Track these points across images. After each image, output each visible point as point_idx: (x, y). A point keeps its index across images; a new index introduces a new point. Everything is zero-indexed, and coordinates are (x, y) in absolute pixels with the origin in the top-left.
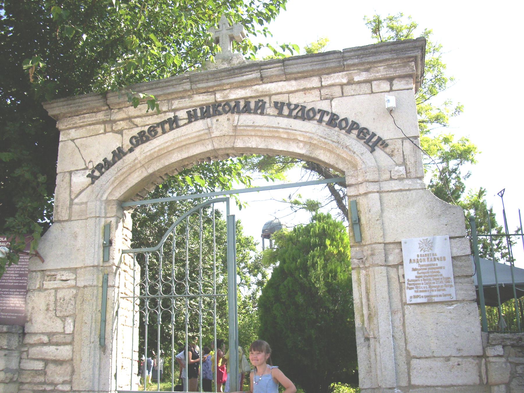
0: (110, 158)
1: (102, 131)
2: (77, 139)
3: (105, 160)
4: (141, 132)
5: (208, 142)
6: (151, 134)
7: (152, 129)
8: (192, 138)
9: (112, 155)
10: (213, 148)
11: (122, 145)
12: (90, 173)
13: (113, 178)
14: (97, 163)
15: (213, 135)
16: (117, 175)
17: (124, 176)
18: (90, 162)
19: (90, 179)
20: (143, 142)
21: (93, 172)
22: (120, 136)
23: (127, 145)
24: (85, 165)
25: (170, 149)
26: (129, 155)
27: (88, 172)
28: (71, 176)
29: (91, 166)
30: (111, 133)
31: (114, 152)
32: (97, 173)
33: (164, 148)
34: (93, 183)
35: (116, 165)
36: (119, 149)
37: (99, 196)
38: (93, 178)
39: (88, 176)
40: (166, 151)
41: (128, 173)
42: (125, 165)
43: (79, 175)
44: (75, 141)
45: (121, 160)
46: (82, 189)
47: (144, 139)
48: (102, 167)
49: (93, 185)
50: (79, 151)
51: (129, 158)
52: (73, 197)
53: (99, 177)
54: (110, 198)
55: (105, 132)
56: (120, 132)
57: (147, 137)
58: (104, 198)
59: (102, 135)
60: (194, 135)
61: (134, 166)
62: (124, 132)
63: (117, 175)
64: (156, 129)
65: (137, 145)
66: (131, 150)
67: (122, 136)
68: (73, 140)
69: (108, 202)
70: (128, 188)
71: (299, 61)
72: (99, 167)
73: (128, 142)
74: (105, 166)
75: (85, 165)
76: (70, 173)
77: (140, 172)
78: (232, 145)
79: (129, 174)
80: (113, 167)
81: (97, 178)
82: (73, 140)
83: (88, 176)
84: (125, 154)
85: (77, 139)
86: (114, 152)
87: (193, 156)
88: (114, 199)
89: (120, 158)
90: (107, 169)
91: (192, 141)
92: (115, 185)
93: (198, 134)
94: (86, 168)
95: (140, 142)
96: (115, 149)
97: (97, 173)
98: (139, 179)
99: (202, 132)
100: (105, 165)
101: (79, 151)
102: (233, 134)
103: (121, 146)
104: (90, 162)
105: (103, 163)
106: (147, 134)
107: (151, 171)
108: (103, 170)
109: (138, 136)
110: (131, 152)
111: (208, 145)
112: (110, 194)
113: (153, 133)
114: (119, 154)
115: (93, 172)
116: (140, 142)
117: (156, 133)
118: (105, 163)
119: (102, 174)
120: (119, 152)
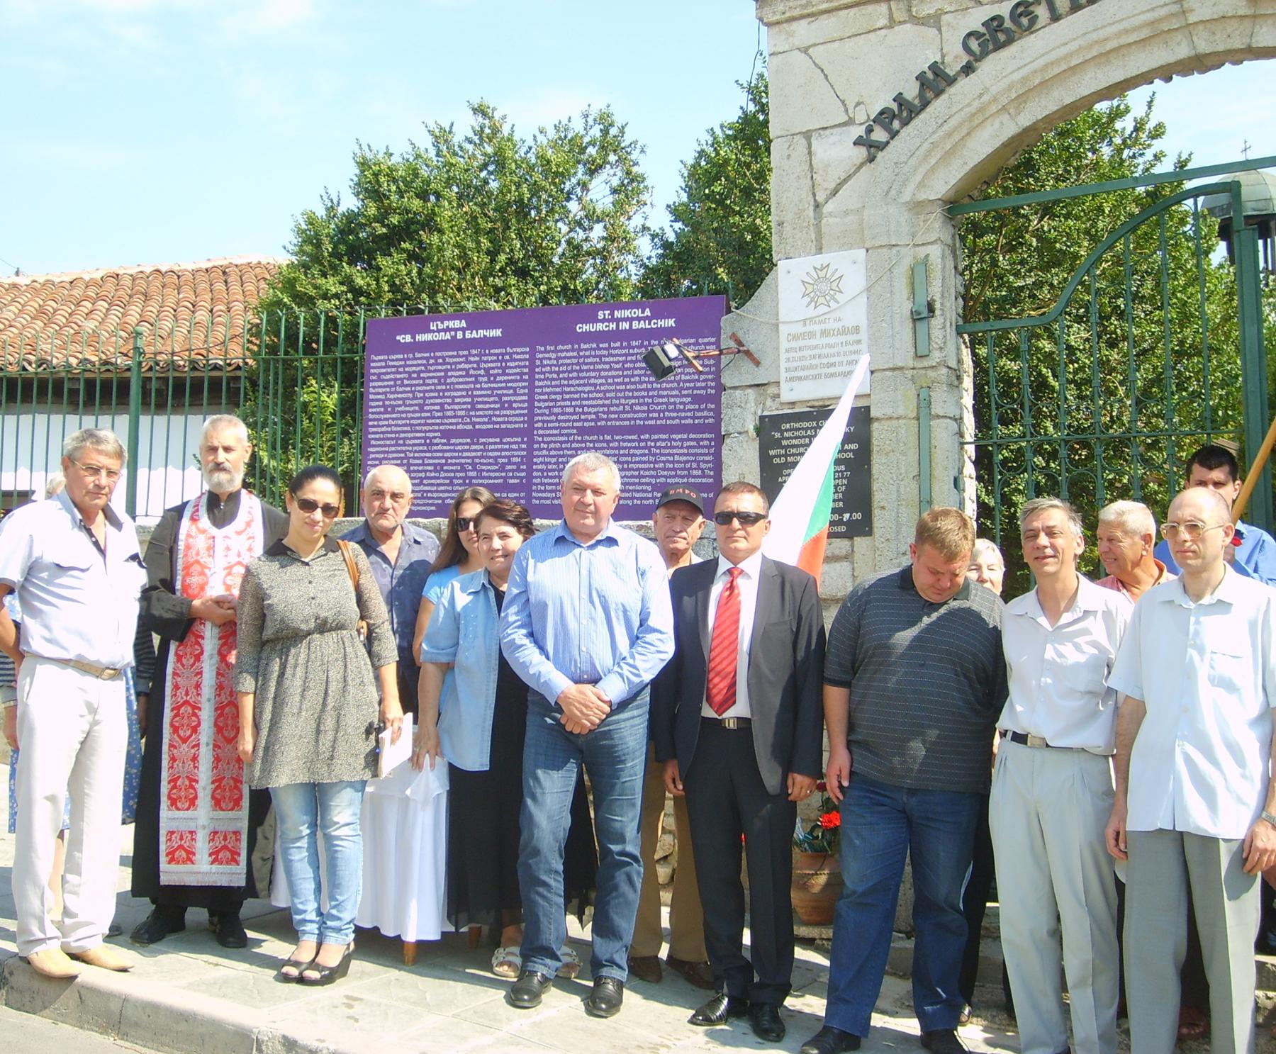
0: (911, 93)
1: (883, 21)
2: (815, 45)
3: (899, 99)
4: (993, 19)
5: (1179, 36)
6: (1019, 25)
7: (1020, 10)
8: (1135, 29)
9: (918, 84)
10: (1193, 53)
11: (943, 56)
12: (863, 134)
13: (926, 146)
14: (878, 109)
15: (1192, 18)
16: (935, 137)
17: (956, 137)
18: (858, 104)
19: (862, 152)
20: (999, 46)
21: (869, 130)
22: (933, 32)
23: (955, 58)
24: (847, 111)
25: (1074, 63)
26: (964, 83)
27: (860, 131)
28: (810, 145)
29: (861, 116)
30: (908, 26)
31: (921, 77)
32: (879, 135)
33: (1057, 62)
34: (871, 159)
35: (930, 109)
36: (934, 67)
37: (893, 192)
38: (872, 148)
39: (858, 142)
40: (1064, 67)
41: (964, 131)
42: (954, 110)
43: (833, 139)
44: (811, 51)
45: (944, 97)
46: (843, 176)
47: (1002, 37)
48: (894, 116)
49: (872, 165)
50: (826, 76)
51: (963, 92)
52: (821, 197)
53: (888, 143)
54: (922, 196)
55: (892, 23)
56: (934, 21)
57: (1007, 32)
58: (906, 197)
59: (883, 32)
60: (1143, 18)
61: (981, 110)
62: (945, 18)
63: (935, 138)
64: (1031, 9)
65: (984, 54)
66: (968, 69)
67: (940, 30)
68: (805, 50)
69: (917, 207)
70: (967, 168)
71: (1236, 252)
72: (884, 118)
73: (959, 49)
74: (901, 113)
75: (847, 111)
76: (807, 135)
77: (997, 124)
78: (1246, 41)
79: (968, 134)
80: (922, 116)
81: (881, 146)
82: (805, 50)
83: (858, 142)
84: (951, 81)
85: (815, 45)
86: (921, 77)
87: (1137, 76)
88: (932, 198)
89: (939, 93)
90: (905, 123)
91: (1131, 39)
92: (933, 161)
93: (1150, 16)
94: (850, 122)
95: (991, 47)
96: (925, 67)
97: (879, 135)
98: (997, 144)
99: (1162, 12)
100: (900, 110)
101: (826, 76)
102: (1249, 13)
103: (938, 59)
104: (858, 104)
105: (895, 106)
106: (1008, 24)
107: (1025, 120)
108: (896, 124)
109: (983, 30)
110: (967, 75)
111: (1179, 44)
112: (921, 185)
113: (1025, 21)
114: (935, 81)
115: (869, 130)
116: (991, 47)
117: (1033, 20)
118: (900, 105)
119: (894, 134)
120: (936, 74)
